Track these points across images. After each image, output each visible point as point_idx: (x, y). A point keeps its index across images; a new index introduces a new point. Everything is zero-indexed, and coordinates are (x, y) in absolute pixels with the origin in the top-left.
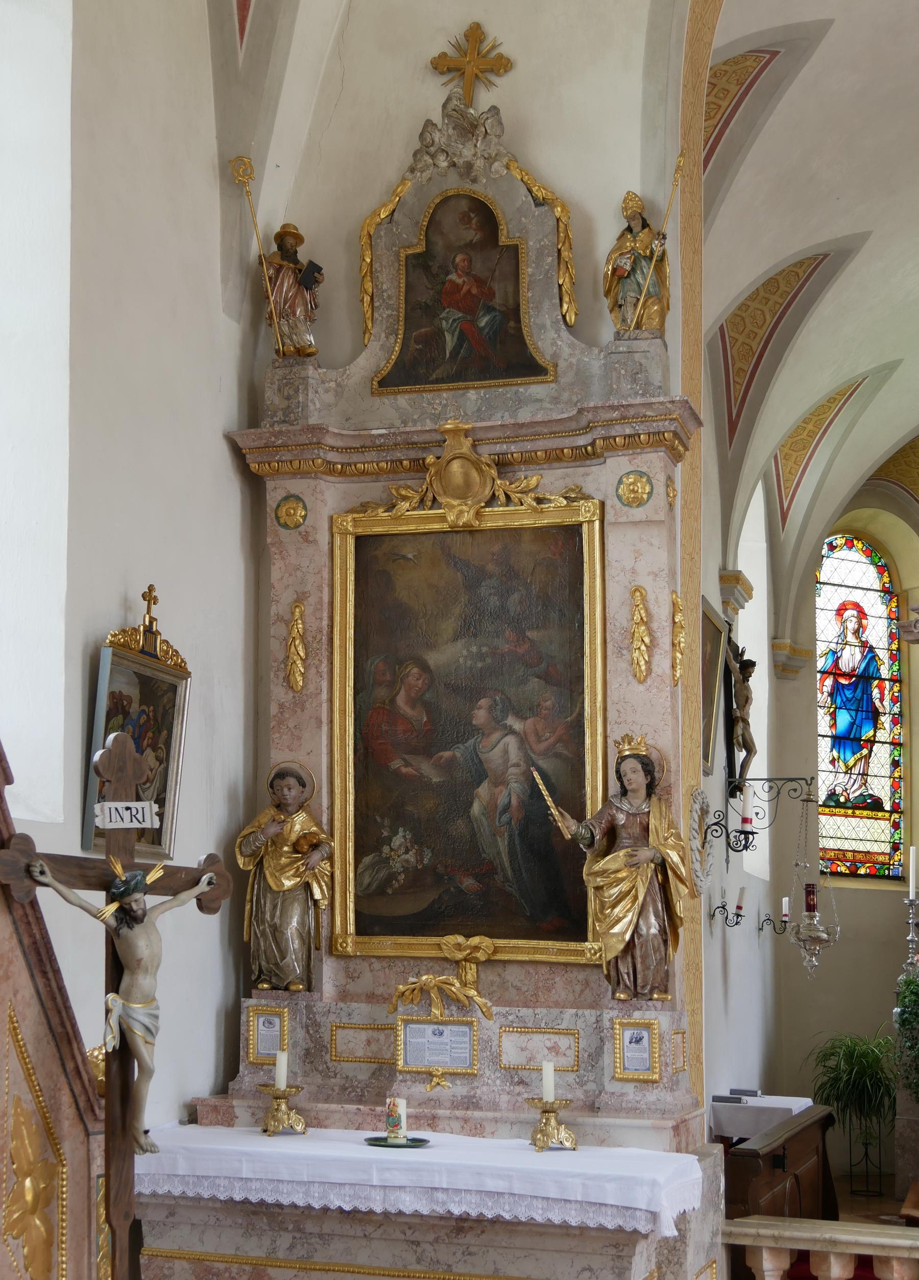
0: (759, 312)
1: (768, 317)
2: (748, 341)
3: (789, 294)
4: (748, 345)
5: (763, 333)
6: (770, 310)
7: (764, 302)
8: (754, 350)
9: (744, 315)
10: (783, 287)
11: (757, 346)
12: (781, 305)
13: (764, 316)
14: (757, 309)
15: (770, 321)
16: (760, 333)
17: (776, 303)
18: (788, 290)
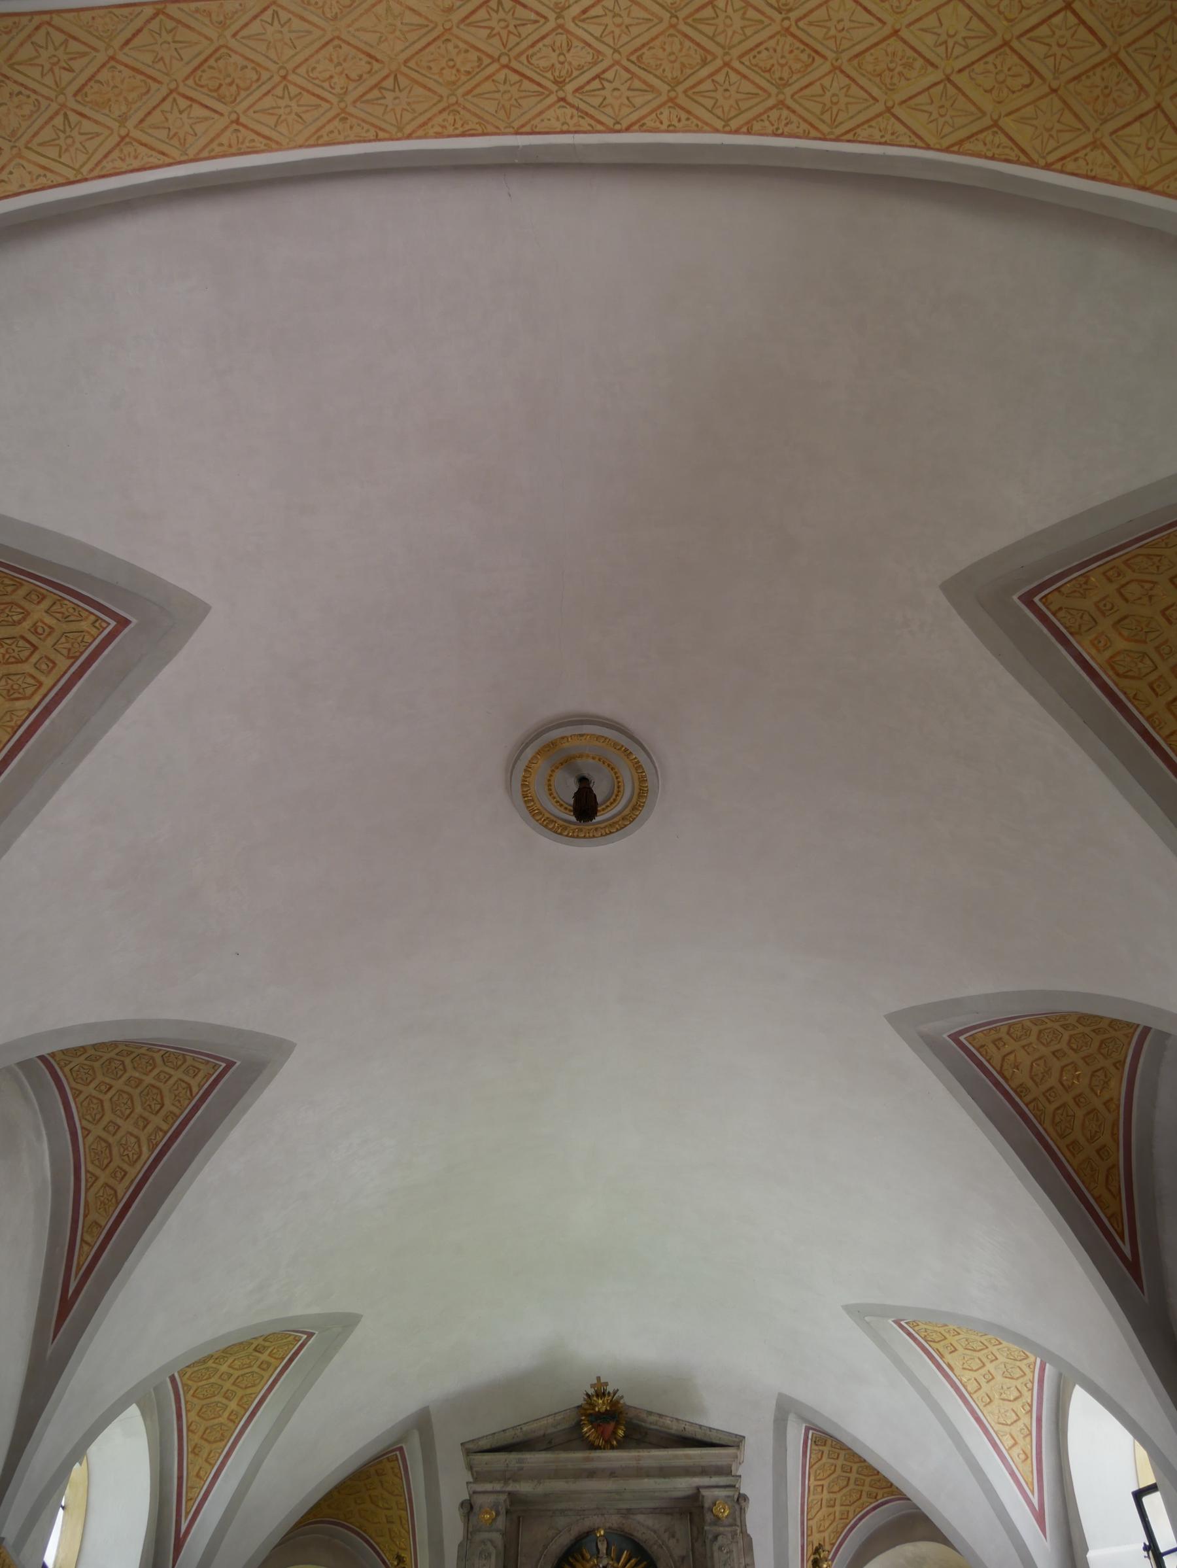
0: (133, 1140)
1: (145, 1149)
2: (112, 1182)
3: (178, 1117)
4: (112, 1188)
5: (135, 1173)
6: (149, 1140)
7: (141, 1124)
8: (120, 1196)
9: (110, 1139)
10: (169, 1106)
11: (124, 1190)
12: (166, 1133)
13: (140, 1146)
14: (132, 1134)
15: (147, 1157)
16: (132, 1172)
17: (159, 1129)
18: (177, 1111)
